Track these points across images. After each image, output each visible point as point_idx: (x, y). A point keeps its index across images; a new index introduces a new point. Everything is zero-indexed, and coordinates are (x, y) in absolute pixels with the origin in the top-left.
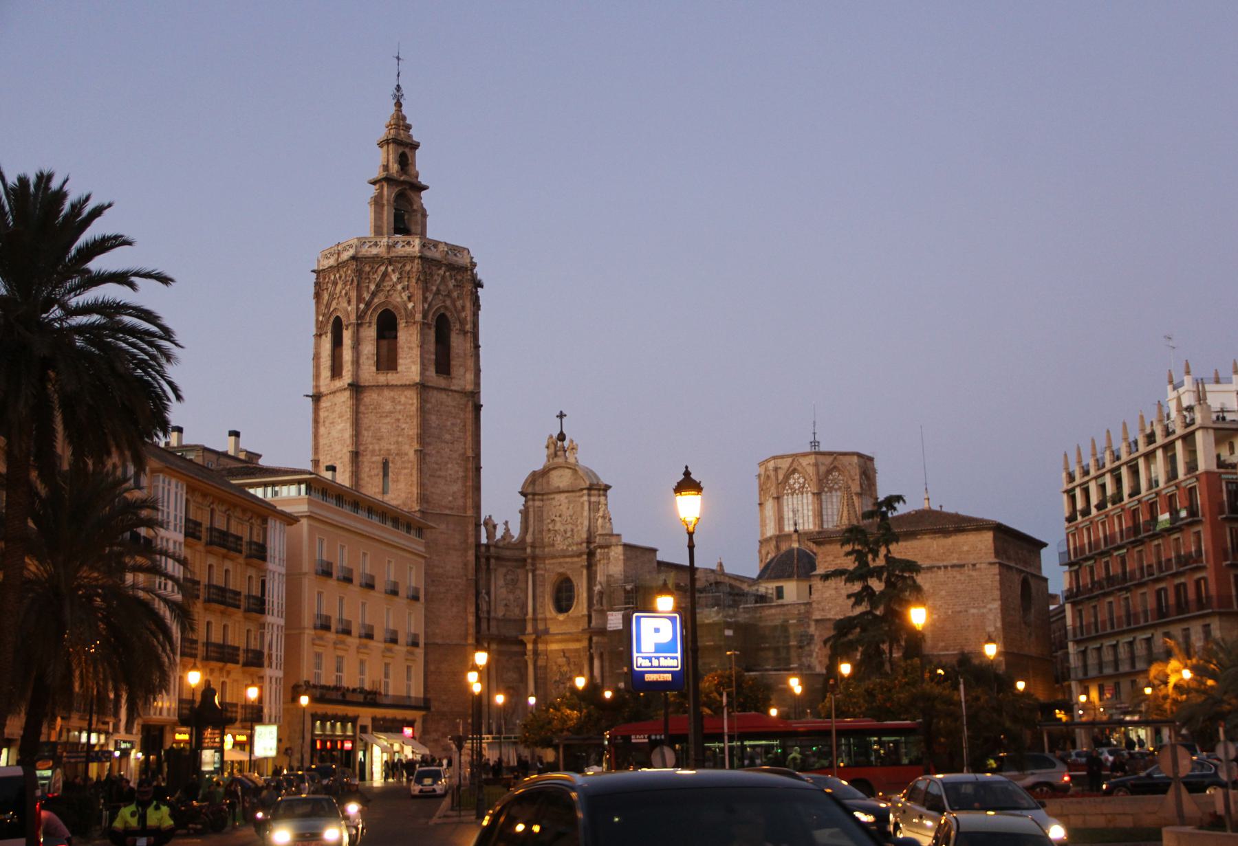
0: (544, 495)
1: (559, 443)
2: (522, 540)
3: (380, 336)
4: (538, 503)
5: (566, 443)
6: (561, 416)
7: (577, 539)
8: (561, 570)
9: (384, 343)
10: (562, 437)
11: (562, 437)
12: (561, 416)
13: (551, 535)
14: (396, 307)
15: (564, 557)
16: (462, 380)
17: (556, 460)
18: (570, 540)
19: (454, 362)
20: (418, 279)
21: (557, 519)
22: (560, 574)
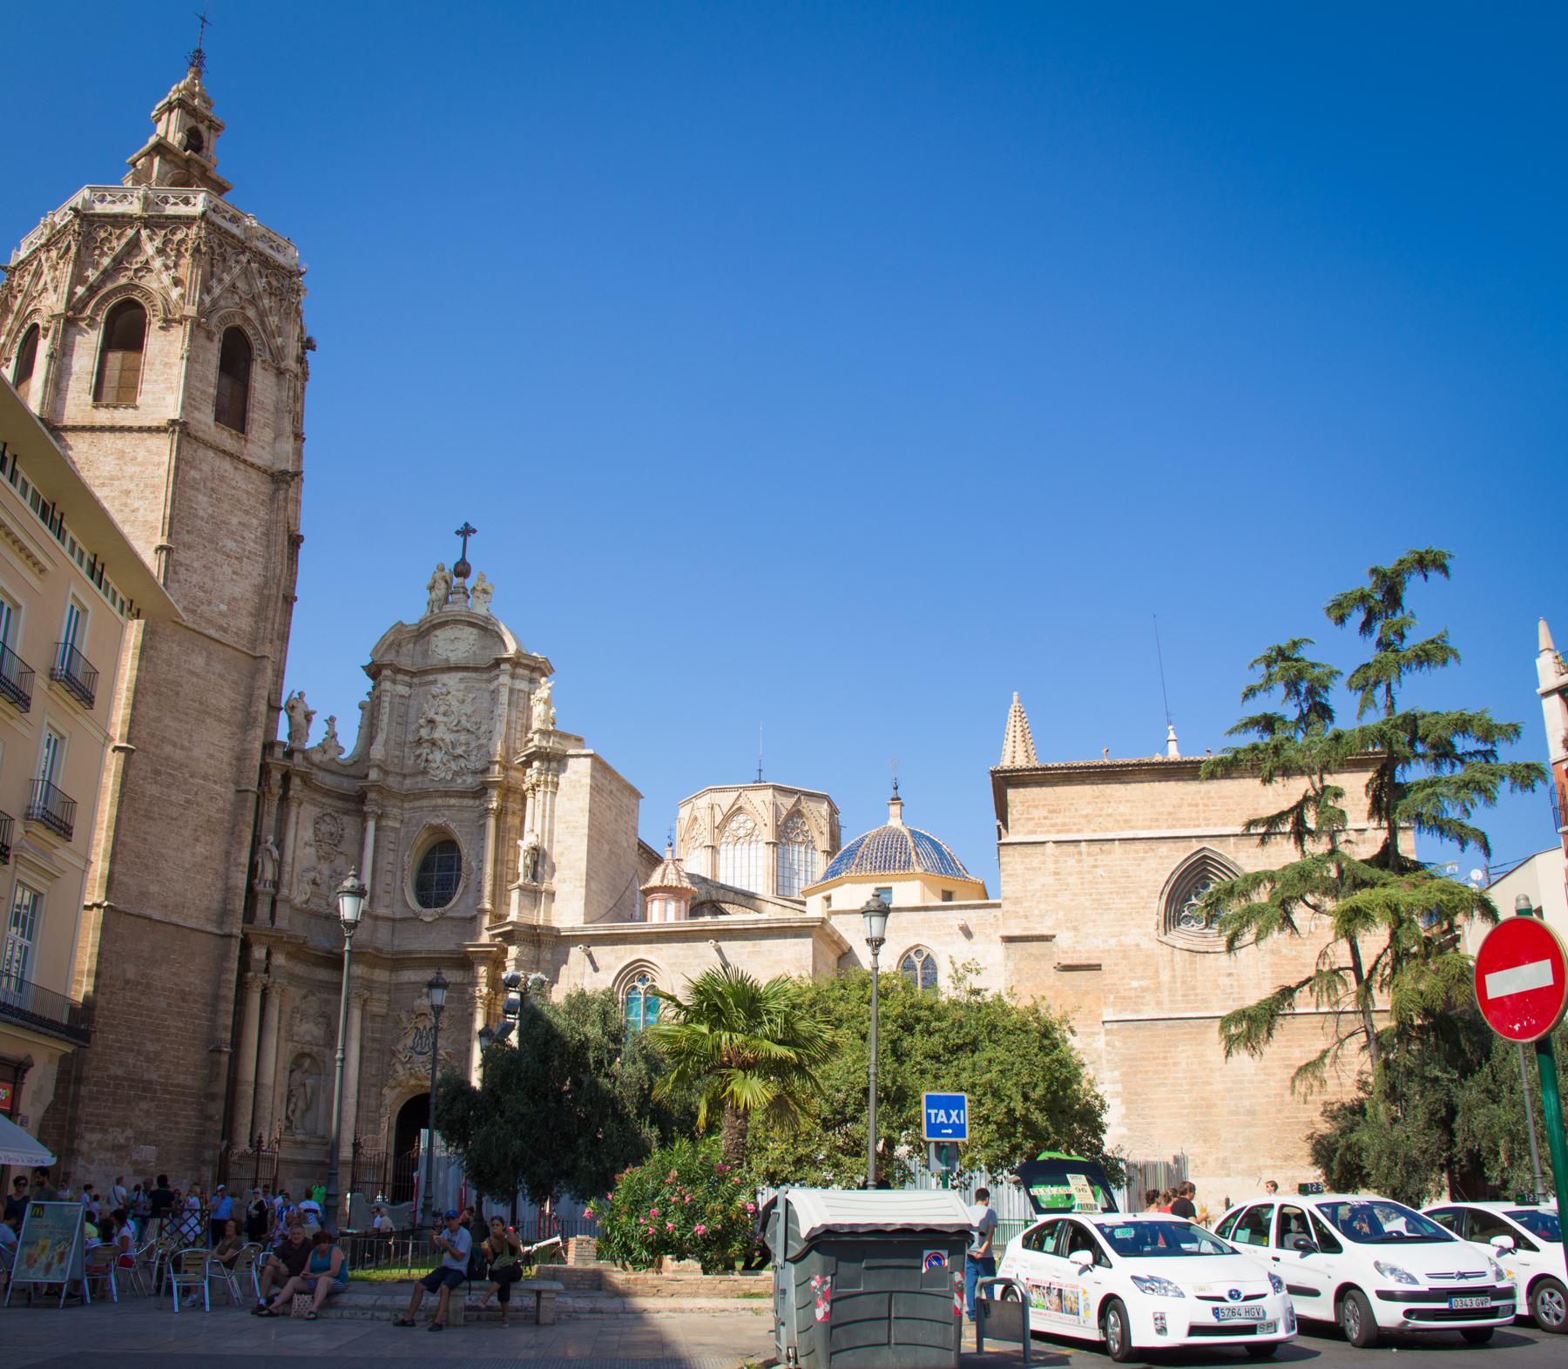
0: (421, 674)
1: (457, 581)
2: (362, 757)
3: (108, 346)
4: (402, 690)
5: (470, 583)
6: (466, 531)
7: (475, 763)
8: (436, 821)
9: (115, 358)
10: (462, 570)
11: (462, 570)
12: (466, 531)
13: (425, 750)
14: (148, 295)
15: (447, 794)
16: (263, 445)
17: (447, 608)
18: (462, 763)
19: (256, 416)
20: (197, 250)
21: (439, 718)
22: (435, 829)
